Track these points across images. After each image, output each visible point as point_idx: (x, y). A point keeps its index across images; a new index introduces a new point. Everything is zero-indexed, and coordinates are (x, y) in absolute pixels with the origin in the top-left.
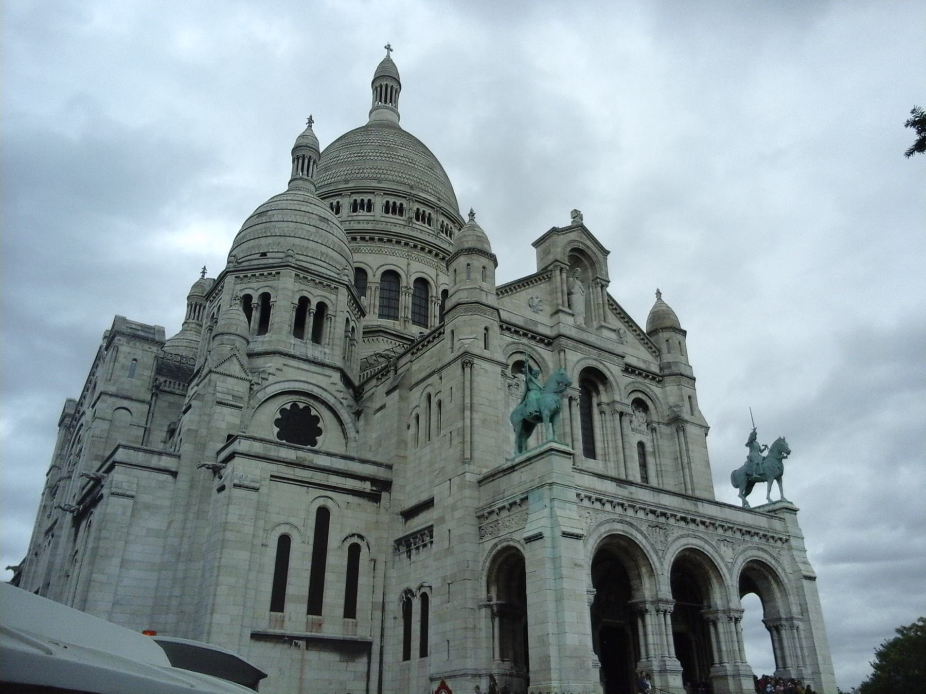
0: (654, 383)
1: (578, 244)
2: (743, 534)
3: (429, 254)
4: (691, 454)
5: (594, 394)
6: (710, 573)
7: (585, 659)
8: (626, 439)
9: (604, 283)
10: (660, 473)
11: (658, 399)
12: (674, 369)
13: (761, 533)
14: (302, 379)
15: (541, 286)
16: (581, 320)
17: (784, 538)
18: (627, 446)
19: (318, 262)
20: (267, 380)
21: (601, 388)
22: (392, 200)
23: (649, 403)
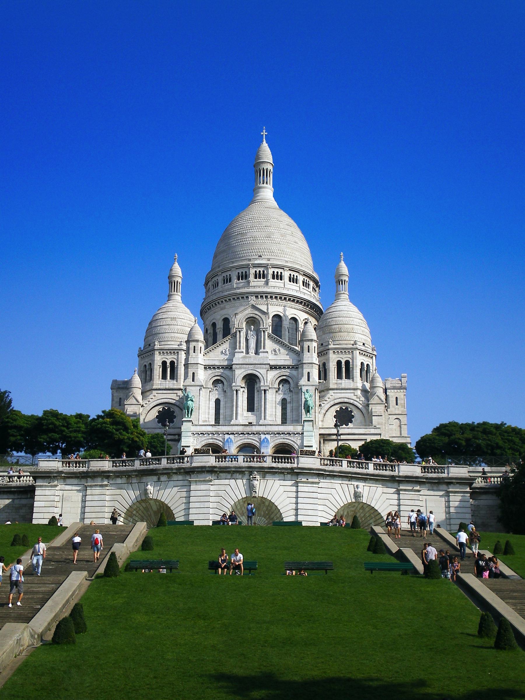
0: (293, 369)
3: (261, 298)
5: (256, 384)
8: (267, 401)
9: (264, 330)
10: (292, 411)
11: (294, 376)
13: (286, 433)
14: (166, 397)
16: (252, 350)
17: (300, 433)
18: (267, 403)
19: (169, 343)
20: (150, 401)
21: (257, 380)
22: (240, 271)
23: (290, 380)
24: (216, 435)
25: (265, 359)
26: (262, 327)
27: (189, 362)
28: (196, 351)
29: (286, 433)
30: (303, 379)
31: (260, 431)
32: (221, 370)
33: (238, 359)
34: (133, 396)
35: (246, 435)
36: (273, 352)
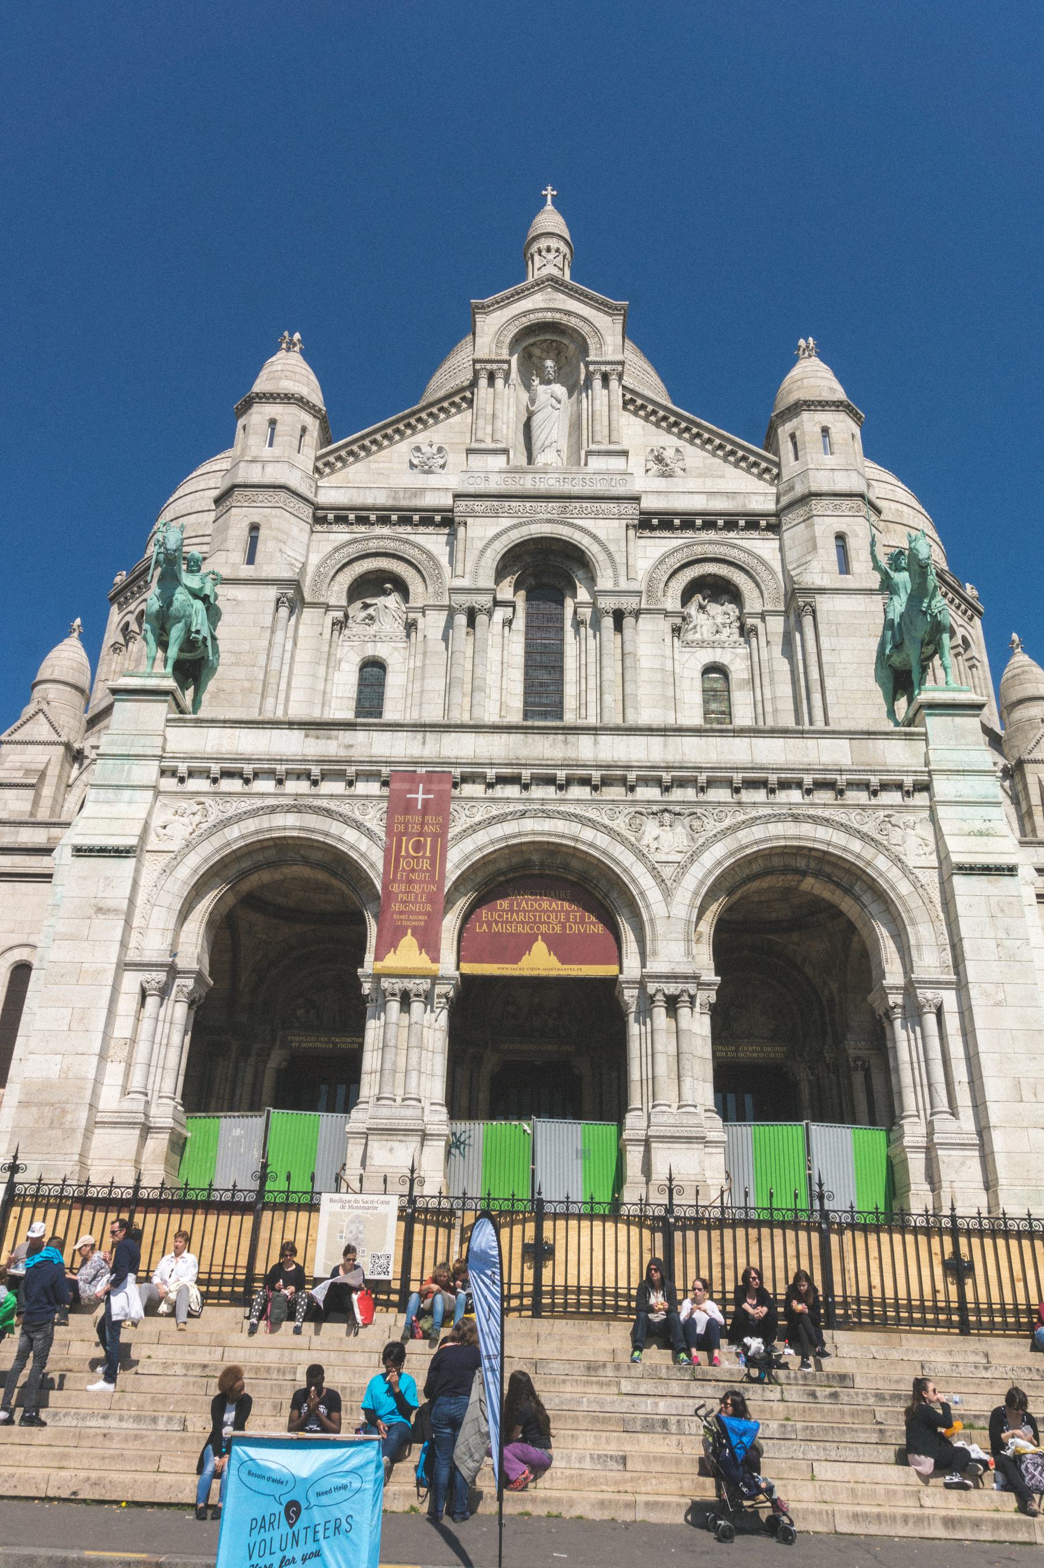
0: (755, 534)
1: (540, 315)
2: (737, 790)
4: (825, 658)
6: (614, 895)
7: (69, 1107)
9: (603, 368)
12: (800, 490)
13: (808, 779)
15: (451, 420)
17: (908, 781)
21: (579, 574)
23: (739, 578)
24: (328, 787)
25: (618, 477)
26: (598, 359)
27: (240, 480)
28: (276, 439)
29: (808, 779)
30: (815, 566)
31: (628, 767)
32: (403, 531)
33: (483, 475)
34: (41, 710)
35: (538, 792)
36: (651, 465)
